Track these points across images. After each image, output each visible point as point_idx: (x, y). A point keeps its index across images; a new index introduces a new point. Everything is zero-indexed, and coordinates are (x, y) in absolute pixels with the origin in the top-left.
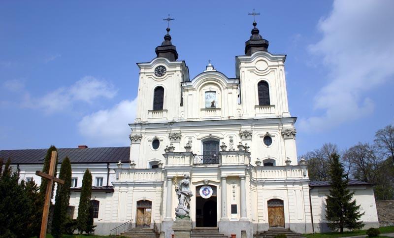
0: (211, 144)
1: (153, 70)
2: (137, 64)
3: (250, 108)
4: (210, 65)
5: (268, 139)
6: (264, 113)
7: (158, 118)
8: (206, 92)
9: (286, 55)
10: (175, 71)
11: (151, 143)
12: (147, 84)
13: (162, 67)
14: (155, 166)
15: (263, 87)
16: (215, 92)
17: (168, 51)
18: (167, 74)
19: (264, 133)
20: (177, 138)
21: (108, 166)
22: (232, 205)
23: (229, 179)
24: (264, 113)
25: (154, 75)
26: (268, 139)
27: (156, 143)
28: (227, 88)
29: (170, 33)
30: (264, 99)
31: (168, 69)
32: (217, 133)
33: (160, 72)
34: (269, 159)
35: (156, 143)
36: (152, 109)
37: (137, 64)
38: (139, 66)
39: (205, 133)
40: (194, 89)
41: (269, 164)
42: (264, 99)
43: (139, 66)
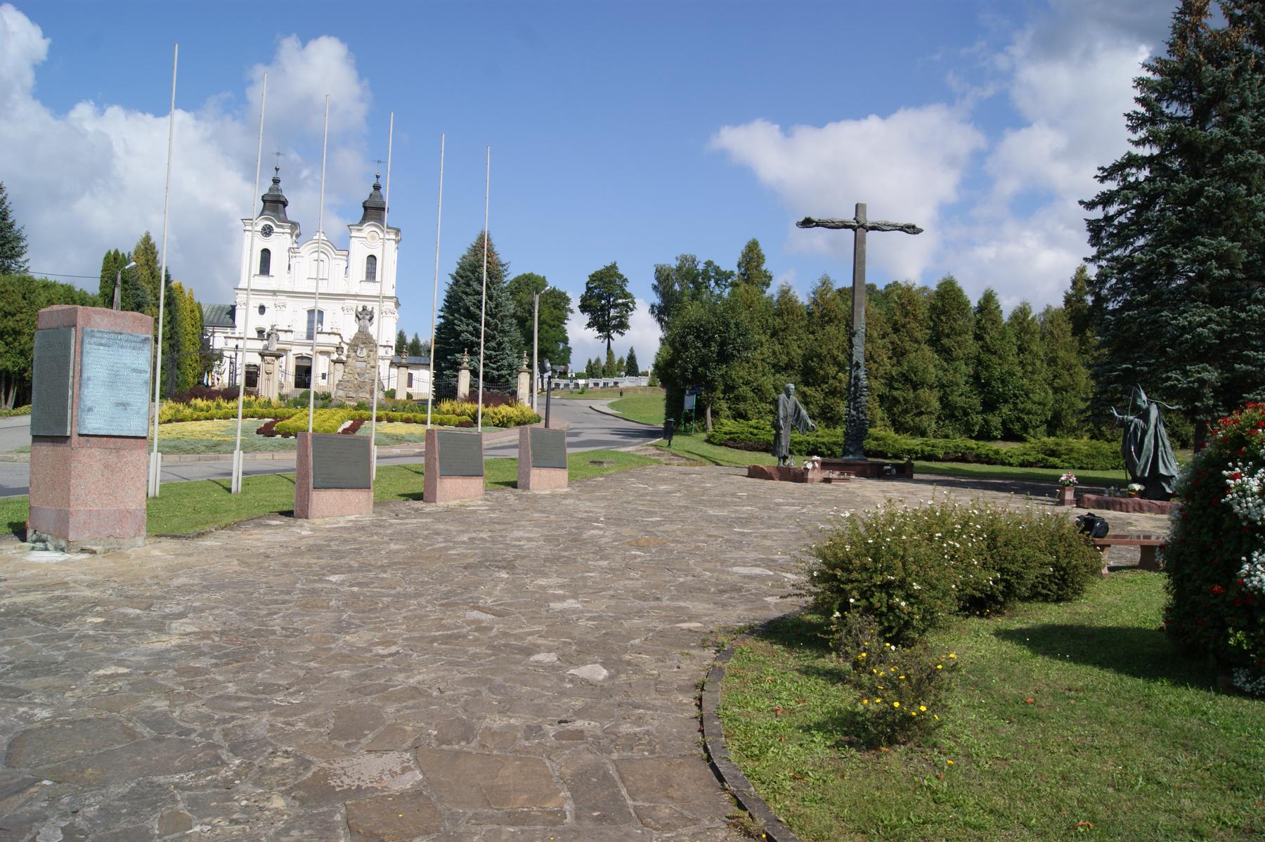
1: (259, 228)
3: (356, 282)
6: (371, 289)
15: (372, 259)
17: (274, 204)
27: (262, 309)
29: (280, 175)
30: (371, 275)
31: (275, 229)
32: (321, 305)
33: (267, 231)
35: (262, 309)
39: (310, 304)
42: (371, 275)
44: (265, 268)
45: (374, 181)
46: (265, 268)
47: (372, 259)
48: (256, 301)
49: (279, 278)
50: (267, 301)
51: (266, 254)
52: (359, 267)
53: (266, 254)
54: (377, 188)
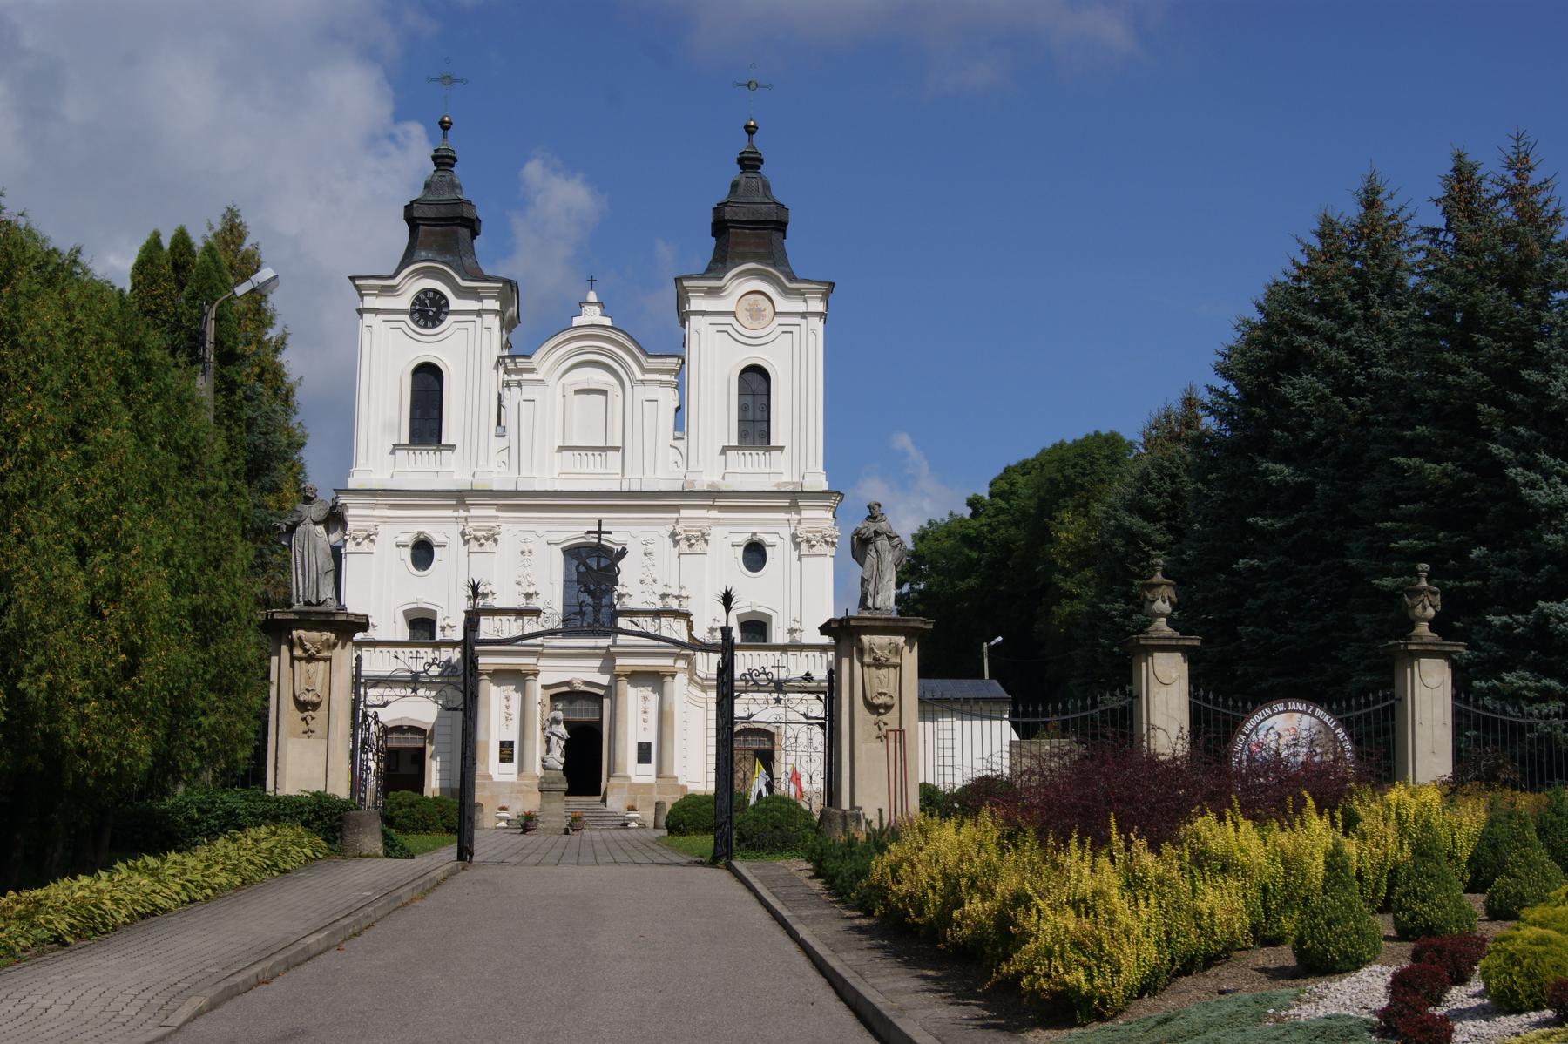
1: (404, 301)
2: (352, 278)
3: (712, 457)
4: (592, 297)
6: (752, 471)
8: (577, 392)
9: (832, 284)
10: (479, 313)
11: (407, 553)
15: (755, 380)
16: (604, 392)
18: (450, 319)
19: (743, 539)
22: (640, 745)
23: (637, 677)
24: (752, 471)
25: (406, 318)
26: (755, 554)
27: (423, 552)
29: (454, 142)
30: (755, 426)
31: (455, 303)
33: (429, 311)
34: (754, 612)
35: (423, 552)
36: (405, 439)
37: (352, 278)
38: (357, 287)
39: (576, 528)
40: (541, 382)
42: (755, 426)
43: (357, 287)
45: (741, 143)
47: (755, 380)
51: (428, 380)
52: (716, 407)
53: (428, 380)
54: (750, 163)
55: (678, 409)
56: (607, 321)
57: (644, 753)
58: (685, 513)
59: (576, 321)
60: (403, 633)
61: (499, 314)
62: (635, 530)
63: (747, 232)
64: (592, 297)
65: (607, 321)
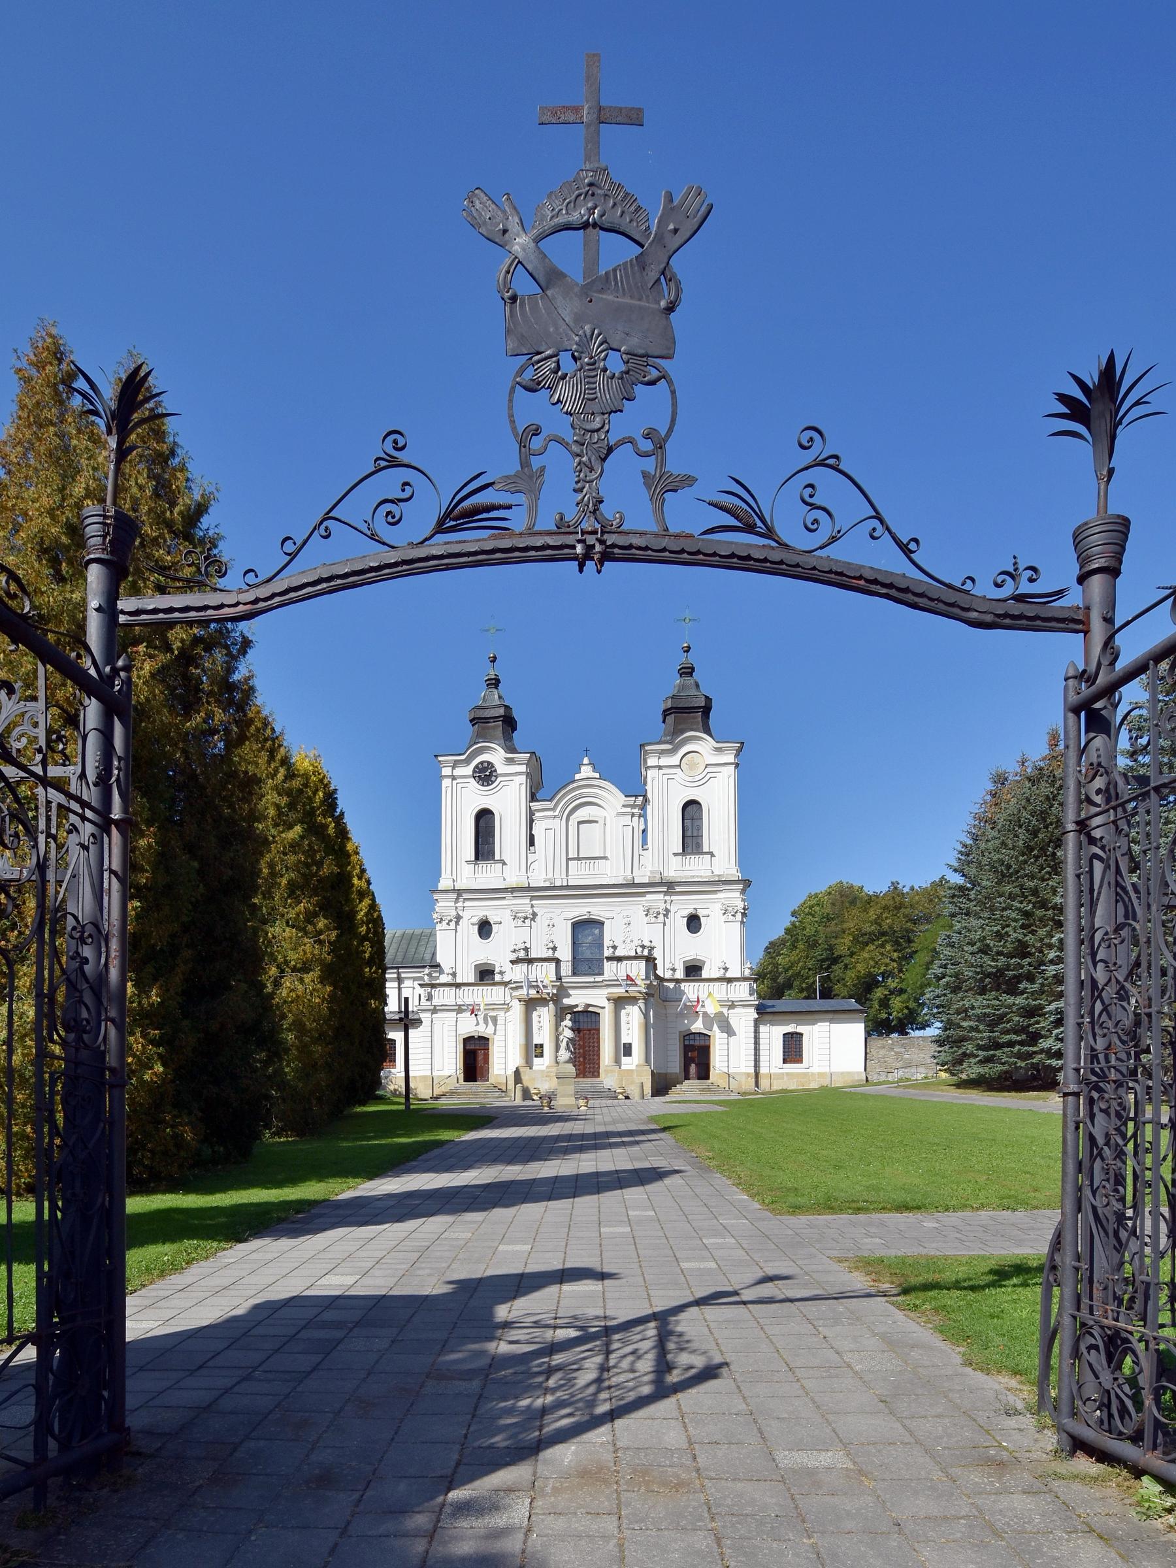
0: (586, 930)
1: (468, 770)
2: (436, 756)
5: (694, 922)
7: (488, 876)
12: (461, 799)
13: (489, 763)
14: (485, 974)
15: (691, 808)
18: (499, 779)
20: (526, 918)
21: (398, 973)
26: (694, 922)
27: (485, 928)
28: (619, 814)
30: (691, 842)
31: (501, 768)
35: (485, 928)
41: (693, 970)
42: (691, 842)
44: (484, 847)
45: (682, 659)
46: (484, 847)
47: (691, 808)
48: (474, 912)
49: (513, 862)
50: (498, 912)
51: (484, 819)
53: (484, 819)
54: (688, 671)
55: (643, 831)
56: (597, 775)
57: (628, 1050)
58: (649, 897)
59: (577, 777)
60: (471, 977)
61: (528, 775)
62: (617, 909)
63: (688, 714)
64: (586, 761)
65: (597, 775)
